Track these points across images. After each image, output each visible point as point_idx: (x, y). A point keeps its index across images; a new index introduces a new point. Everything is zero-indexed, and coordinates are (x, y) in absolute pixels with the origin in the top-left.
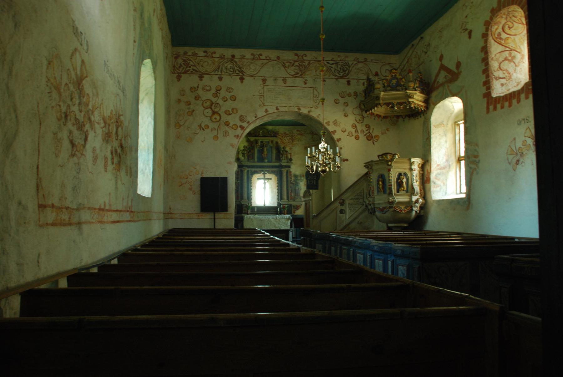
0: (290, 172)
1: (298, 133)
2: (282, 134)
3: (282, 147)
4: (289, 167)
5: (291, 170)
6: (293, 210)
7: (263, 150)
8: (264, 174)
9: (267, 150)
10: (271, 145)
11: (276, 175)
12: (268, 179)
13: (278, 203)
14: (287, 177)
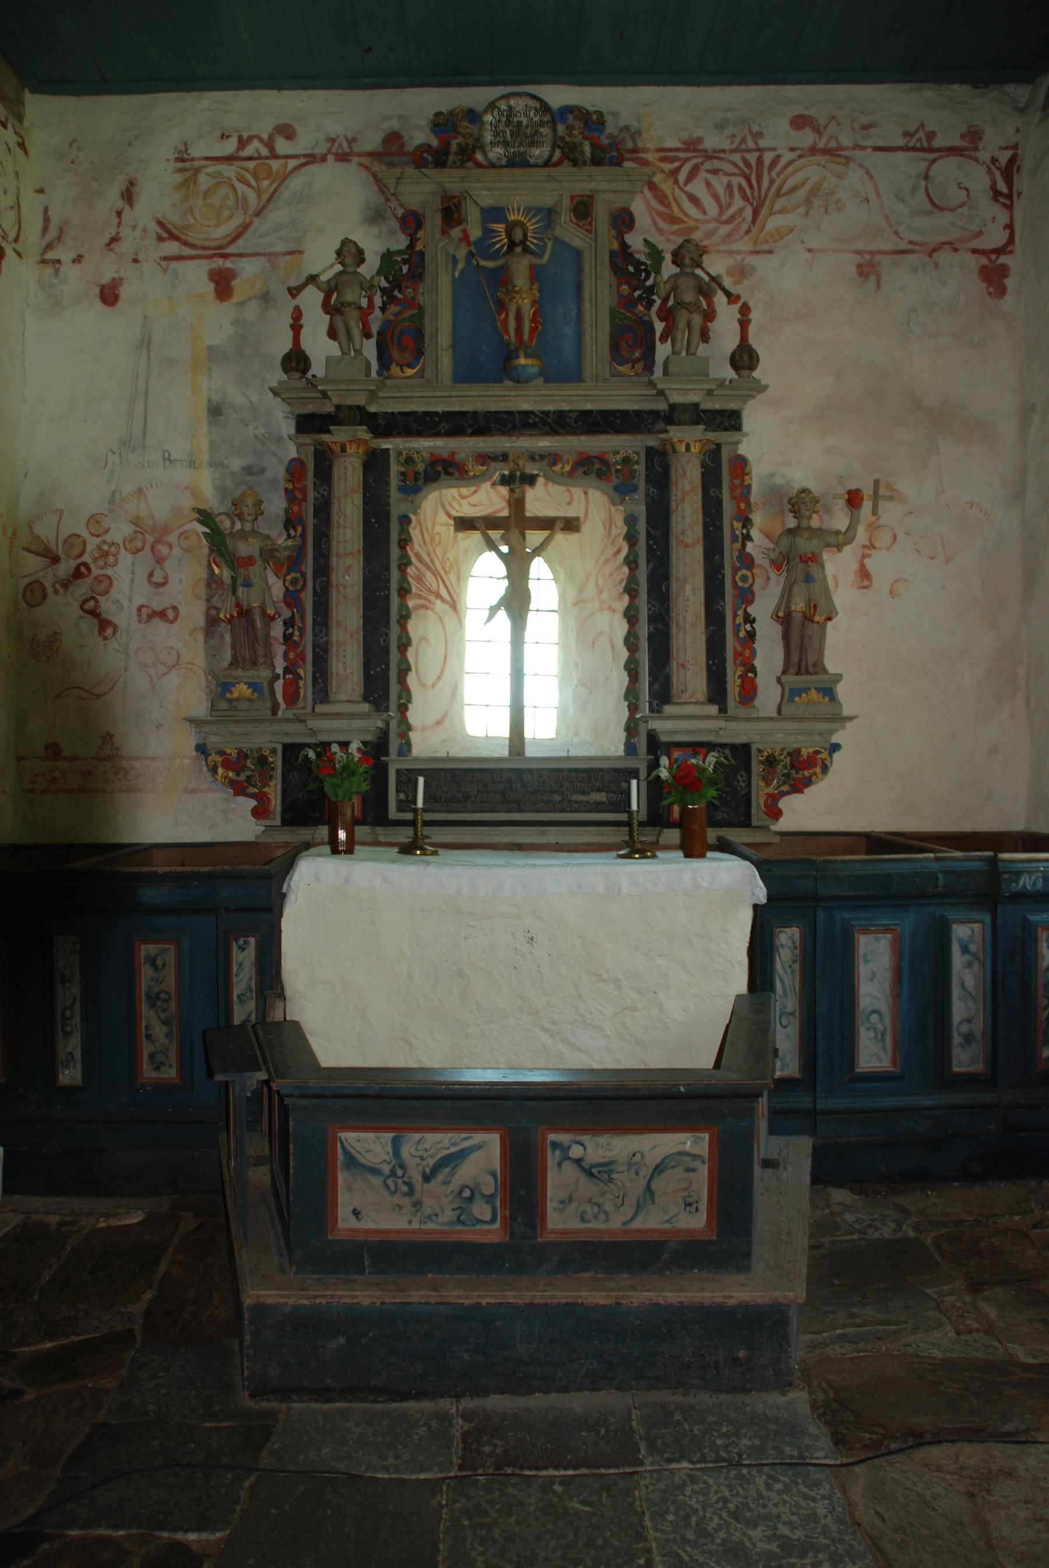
0: (740, 465)
1: (806, 138)
2: (666, 154)
3: (667, 247)
4: (731, 421)
5: (742, 450)
6: (760, 792)
7: (502, 279)
8: (517, 481)
9: (535, 274)
10: (577, 239)
11: (622, 491)
12: (547, 524)
13: (631, 729)
14: (712, 510)
